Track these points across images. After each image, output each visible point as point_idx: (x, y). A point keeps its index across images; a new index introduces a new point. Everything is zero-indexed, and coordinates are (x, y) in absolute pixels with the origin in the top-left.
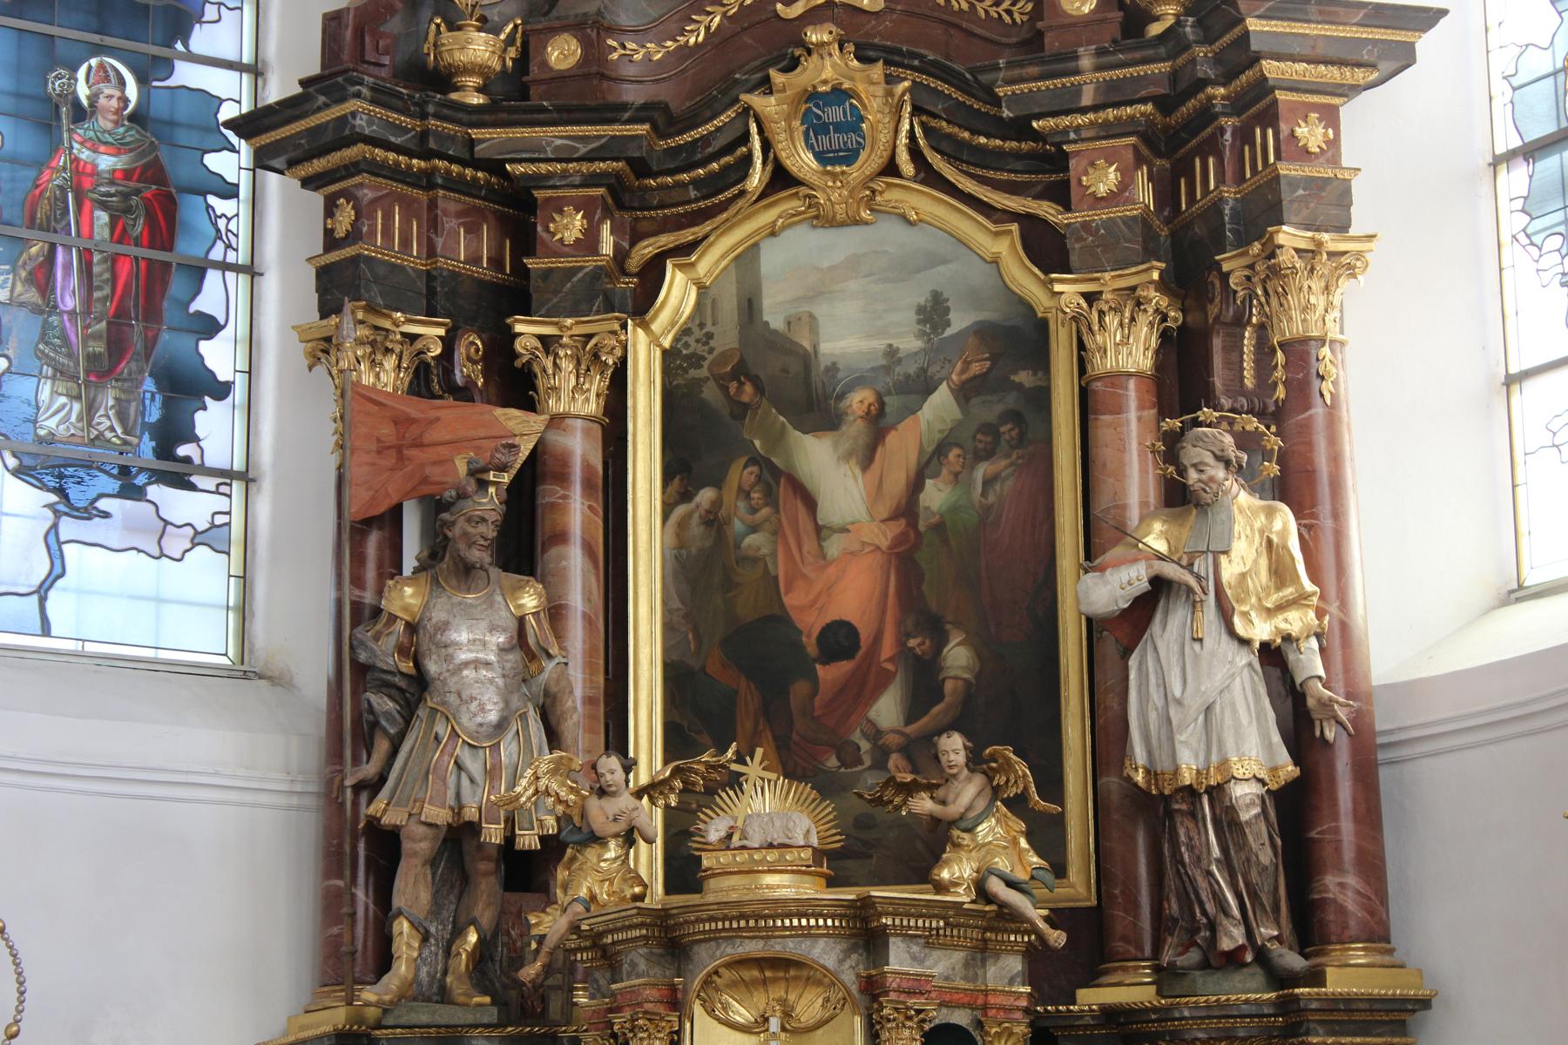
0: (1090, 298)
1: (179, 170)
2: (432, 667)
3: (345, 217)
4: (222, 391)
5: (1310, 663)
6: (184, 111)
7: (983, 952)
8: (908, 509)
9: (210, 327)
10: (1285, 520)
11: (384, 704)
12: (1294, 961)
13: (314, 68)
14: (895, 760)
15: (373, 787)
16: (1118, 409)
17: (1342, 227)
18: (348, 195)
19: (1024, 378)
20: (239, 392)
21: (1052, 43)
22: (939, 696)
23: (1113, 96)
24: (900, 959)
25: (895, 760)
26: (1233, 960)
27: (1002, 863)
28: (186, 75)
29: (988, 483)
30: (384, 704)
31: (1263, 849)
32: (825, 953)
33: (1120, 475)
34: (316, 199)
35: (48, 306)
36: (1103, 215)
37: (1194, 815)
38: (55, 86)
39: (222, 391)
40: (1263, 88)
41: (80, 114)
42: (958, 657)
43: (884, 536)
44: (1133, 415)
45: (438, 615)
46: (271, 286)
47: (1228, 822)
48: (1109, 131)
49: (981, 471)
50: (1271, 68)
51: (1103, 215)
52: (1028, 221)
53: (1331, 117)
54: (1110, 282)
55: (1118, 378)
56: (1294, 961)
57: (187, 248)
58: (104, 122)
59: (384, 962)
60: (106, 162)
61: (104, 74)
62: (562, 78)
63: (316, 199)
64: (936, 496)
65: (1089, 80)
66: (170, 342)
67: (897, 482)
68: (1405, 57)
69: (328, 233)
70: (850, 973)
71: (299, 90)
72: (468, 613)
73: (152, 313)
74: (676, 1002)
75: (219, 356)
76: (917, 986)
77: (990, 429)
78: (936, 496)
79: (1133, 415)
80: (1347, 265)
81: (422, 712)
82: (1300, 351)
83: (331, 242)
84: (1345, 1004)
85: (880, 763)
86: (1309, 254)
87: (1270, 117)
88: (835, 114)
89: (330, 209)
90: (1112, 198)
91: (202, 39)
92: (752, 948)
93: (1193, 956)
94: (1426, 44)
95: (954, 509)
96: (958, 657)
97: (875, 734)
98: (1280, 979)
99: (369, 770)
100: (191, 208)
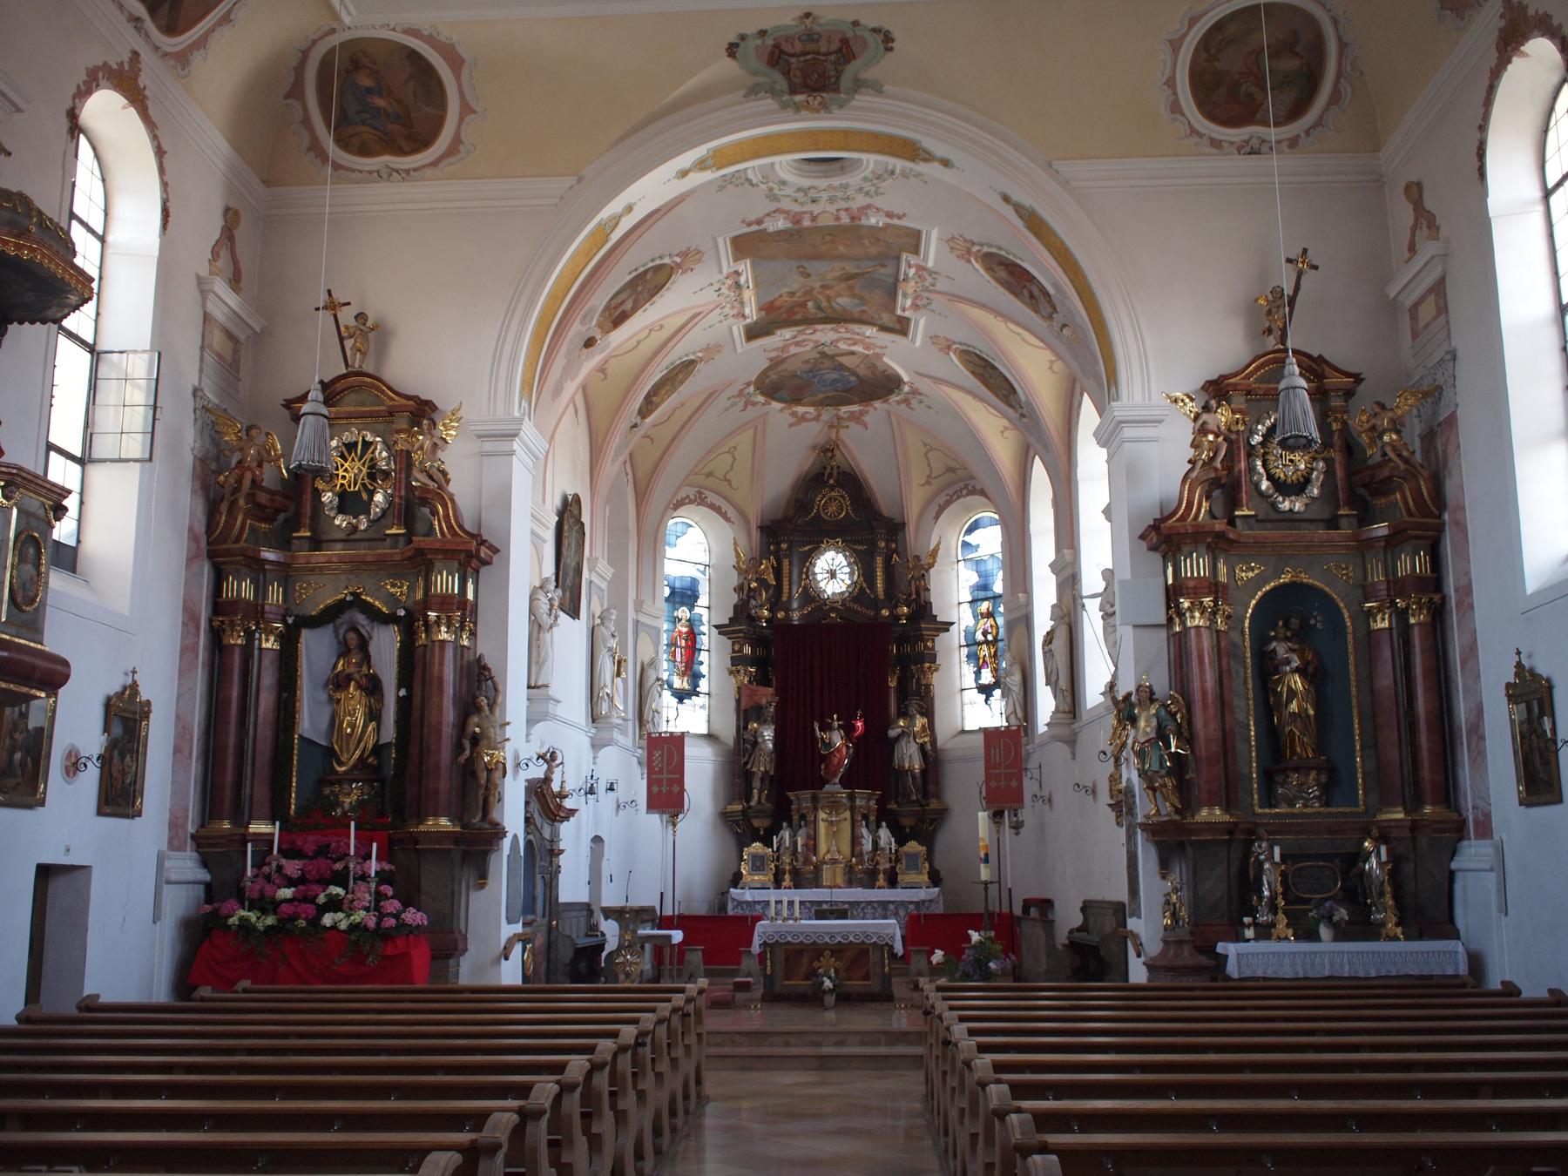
1: (696, 631)
2: (760, 740)
3: (737, 647)
4: (704, 676)
5: (929, 747)
6: (697, 618)
7: (869, 800)
9: (702, 663)
10: (925, 720)
11: (748, 746)
12: (923, 802)
13: (731, 615)
15: (746, 763)
17: (935, 662)
18: (738, 642)
20: (707, 677)
24: (858, 802)
26: (913, 802)
28: (697, 610)
30: (748, 746)
31: (919, 781)
32: (845, 801)
34: (730, 642)
35: (675, 661)
37: (907, 775)
38: (675, 614)
39: (704, 676)
40: (922, 635)
41: (680, 620)
45: (761, 730)
46: (713, 652)
47: (914, 777)
50: (924, 633)
53: (933, 641)
56: (923, 802)
57: (698, 647)
58: (683, 621)
59: (748, 799)
60: (685, 630)
61: (683, 611)
62: (780, 620)
63: (730, 642)
66: (696, 667)
68: (948, 630)
69: (733, 649)
70: (849, 804)
71: (727, 622)
72: (766, 729)
73: (693, 662)
74: (816, 809)
75: (704, 669)
76: (861, 807)
80: (936, 670)
81: (757, 749)
82: (928, 686)
83: (734, 651)
84: (932, 810)
86: (929, 668)
87: (923, 640)
89: (733, 644)
91: (699, 602)
92: (831, 799)
93: (905, 801)
94: (951, 628)
98: (921, 806)
99: (745, 759)
100: (698, 637)
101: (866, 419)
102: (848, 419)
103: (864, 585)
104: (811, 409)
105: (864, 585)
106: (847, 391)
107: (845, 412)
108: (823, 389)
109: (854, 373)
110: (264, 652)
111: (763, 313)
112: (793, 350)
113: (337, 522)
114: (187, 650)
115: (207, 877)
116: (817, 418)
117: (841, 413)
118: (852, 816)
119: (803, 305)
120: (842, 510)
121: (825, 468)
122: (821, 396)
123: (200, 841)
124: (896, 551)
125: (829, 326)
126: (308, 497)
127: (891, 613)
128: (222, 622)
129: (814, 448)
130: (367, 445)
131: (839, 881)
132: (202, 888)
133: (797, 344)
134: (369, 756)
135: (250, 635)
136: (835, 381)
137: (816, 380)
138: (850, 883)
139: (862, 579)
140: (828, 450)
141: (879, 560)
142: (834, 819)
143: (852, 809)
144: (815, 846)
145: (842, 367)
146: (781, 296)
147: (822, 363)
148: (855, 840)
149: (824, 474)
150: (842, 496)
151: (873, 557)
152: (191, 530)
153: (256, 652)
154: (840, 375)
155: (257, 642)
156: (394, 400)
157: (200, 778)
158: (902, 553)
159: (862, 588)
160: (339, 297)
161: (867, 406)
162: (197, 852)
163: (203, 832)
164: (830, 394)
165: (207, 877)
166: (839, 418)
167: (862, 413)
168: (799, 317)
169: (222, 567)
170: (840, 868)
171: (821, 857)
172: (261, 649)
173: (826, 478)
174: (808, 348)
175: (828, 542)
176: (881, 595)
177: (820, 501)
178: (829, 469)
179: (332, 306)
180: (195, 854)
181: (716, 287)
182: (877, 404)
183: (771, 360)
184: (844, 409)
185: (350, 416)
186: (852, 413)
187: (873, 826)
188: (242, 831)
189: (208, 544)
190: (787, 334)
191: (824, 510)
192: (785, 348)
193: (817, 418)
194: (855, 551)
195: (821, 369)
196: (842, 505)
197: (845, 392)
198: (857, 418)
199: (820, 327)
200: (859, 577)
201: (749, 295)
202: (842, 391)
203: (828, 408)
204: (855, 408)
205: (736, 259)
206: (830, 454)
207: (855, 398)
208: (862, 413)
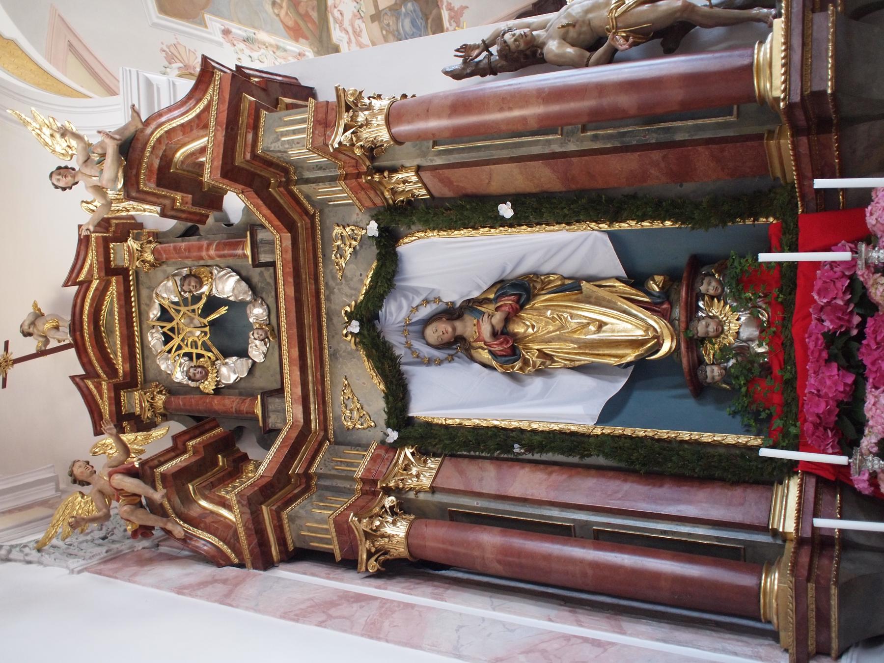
101: (456, 5)
106: (426, 17)
107: (451, 25)
110: (439, 483)
111: (301, 40)
123: (812, 647)
126: (217, 403)
128: (370, 555)
130: (165, 315)
134: (648, 293)
136: (413, 23)
146: (278, 15)
147: (388, 25)
152: (181, 590)
153: (439, 498)
155: (422, 496)
156: (91, 265)
157: (663, 630)
162: (839, 657)
163: (788, 636)
167: (450, 9)
168: (314, 15)
169: (291, 547)
172: (433, 490)
174: (363, 26)
186: (451, 18)
188: (790, 547)
189: (241, 565)
190: (337, 35)
195: (398, 30)
197: (427, 19)
201: (262, 36)
205: (203, 24)
207: (434, 12)
208: (450, 9)
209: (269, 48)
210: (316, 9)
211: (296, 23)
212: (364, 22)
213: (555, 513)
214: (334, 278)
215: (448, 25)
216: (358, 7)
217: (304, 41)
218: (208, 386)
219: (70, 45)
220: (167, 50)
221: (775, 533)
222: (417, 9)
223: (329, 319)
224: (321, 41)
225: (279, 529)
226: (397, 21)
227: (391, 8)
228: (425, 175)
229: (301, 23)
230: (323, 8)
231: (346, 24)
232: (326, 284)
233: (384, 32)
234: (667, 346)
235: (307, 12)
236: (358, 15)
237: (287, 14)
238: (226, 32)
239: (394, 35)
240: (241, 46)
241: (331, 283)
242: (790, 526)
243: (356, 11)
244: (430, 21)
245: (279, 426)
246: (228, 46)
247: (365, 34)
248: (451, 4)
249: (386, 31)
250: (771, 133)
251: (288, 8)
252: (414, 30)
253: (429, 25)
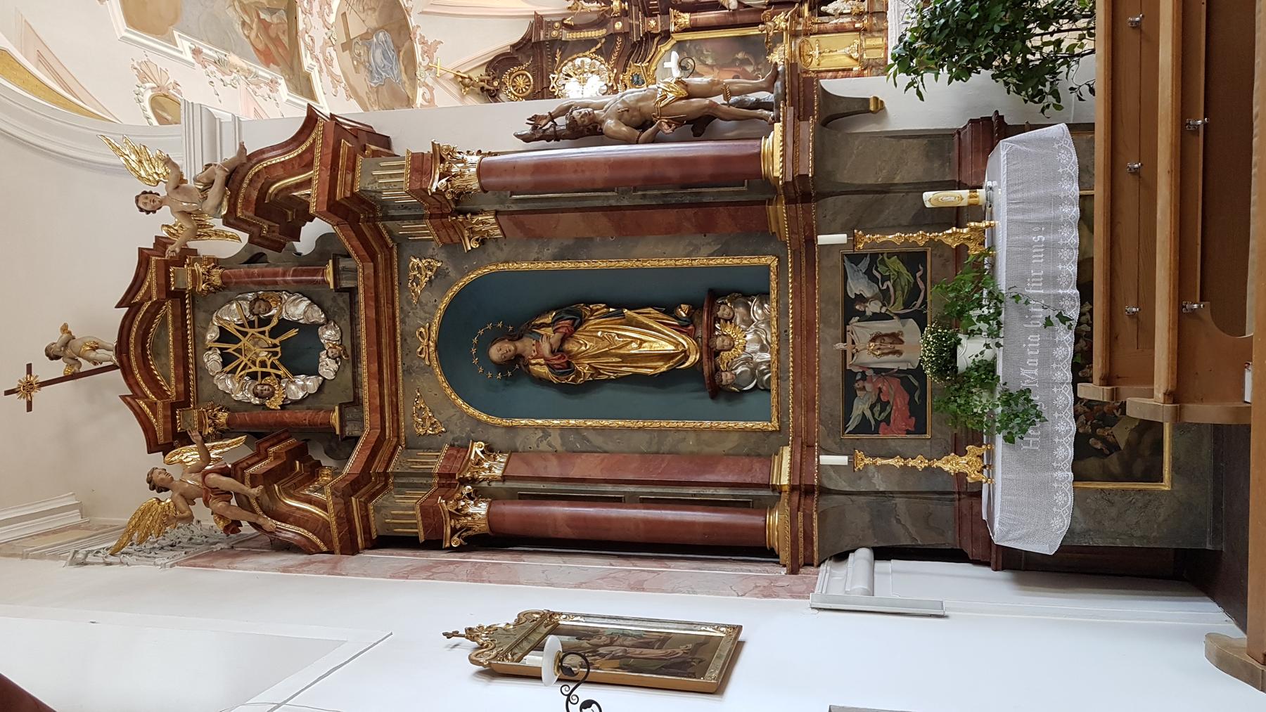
0: (675, 24)
8: (711, 67)
14: (760, 67)
16: (696, 19)
19: (688, 45)
21: (627, 30)
22: (748, 59)
23: (637, 18)
24: (800, 28)
25: (760, 67)
27: (782, 17)
29: (707, 51)
32: (799, 41)
33: (708, 18)
36: (660, 24)
42: (740, 56)
43: (716, 71)
44: (698, 17)
48: (643, 21)
49: (705, 52)
51: (660, 24)
52: (657, 45)
54: (673, 20)
55: (690, 20)
64: (709, 61)
65: (635, 22)
67: (706, 69)
70: (802, 38)
77: (697, 51)
78: (709, 61)
79: (698, 17)
85: (760, 70)
88: (635, 79)
90: (656, 22)
92: (797, 53)
95: (712, 58)
96: (740, 56)
97: (754, 71)
102: (431, 58)
103: (593, 50)
104: (420, 91)
105: (593, 50)
108: (395, 72)
109: (375, 31)
110: (509, 473)
112: (337, 70)
113: (330, 376)
114: (476, 576)
115: (863, 554)
116: (431, 89)
117: (424, 64)
118: (815, 34)
119: (265, 26)
120: (523, 75)
121: (482, 88)
122: (404, 77)
123: (801, 561)
124: (562, 22)
125: (301, 17)
126: (287, 416)
127: (618, 18)
128: (454, 531)
129: (463, 96)
130: (225, 336)
131: (879, 42)
132: (881, 566)
133: (329, 63)
134: (677, 318)
135: (476, 496)
137: (383, 74)
138: (884, 31)
139: (587, 53)
140: (464, 83)
141: (568, 36)
142: (817, 52)
143: (808, 33)
144: (843, 70)
145: (366, 38)
146: (248, 37)
148: (839, 30)
149: (488, 90)
150: (510, 74)
151: (566, 42)
152: (285, 570)
153: (508, 484)
154: (377, 46)
155: (493, 484)
156: (149, 287)
158: (565, 16)
159: (598, 52)
160: (17, 377)
161: (415, 34)
162: (819, 566)
163: (785, 555)
164: (403, 68)
165: (863, 554)
166: (429, 68)
168: (285, 39)
169: (374, 536)
170: (870, 42)
171: (855, 63)
172: (504, 478)
173: (492, 88)
174: (334, 54)
175: (553, 87)
176: (603, 32)
177: (515, 95)
178: (483, 83)
179: (28, 388)
180: (823, 567)
181: (218, 84)
182: (413, 21)
183: (349, 97)
184: (419, 58)
185: (182, 361)
186: (424, 52)
187: (825, 19)
190: (307, 61)
191: (523, 92)
192: (335, 80)
193: (431, 89)
194: (561, 62)
196: (519, 75)
197: (399, 51)
198: (429, 51)
199: (301, 26)
200: (586, 56)
201: (234, 59)
202: (399, 56)
203: (418, 73)
204: (418, 49)
206: (467, 80)
207: (407, 44)
209: (241, 73)
210: (286, 33)
211: (266, 45)
212: (335, 50)
213: (609, 488)
214: (410, 303)
215: (421, 60)
216: (329, 34)
217: (275, 67)
218: (275, 403)
219: (40, 55)
220: (139, 68)
221: (774, 488)
222: (389, 40)
223: (404, 340)
224: (292, 68)
225: (365, 518)
226: (368, 51)
227: (362, 37)
228: (502, 219)
229: (271, 47)
230: (294, 33)
231: (317, 51)
232: (401, 308)
233: (355, 63)
234: (693, 358)
235: (277, 35)
236: (329, 42)
237: (257, 36)
238: (196, 52)
239: (365, 67)
240: (212, 68)
241: (406, 308)
242: (785, 481)
243: (326, 38)
244: (401, 54)
245: (356, 433)
246: (198, 66)
247: (335, 62)
248: (424, 37)
249: (357, 61)
250: (770, 202)
251: (258, 29)
252: (385, 62)
253: (401, 58)
